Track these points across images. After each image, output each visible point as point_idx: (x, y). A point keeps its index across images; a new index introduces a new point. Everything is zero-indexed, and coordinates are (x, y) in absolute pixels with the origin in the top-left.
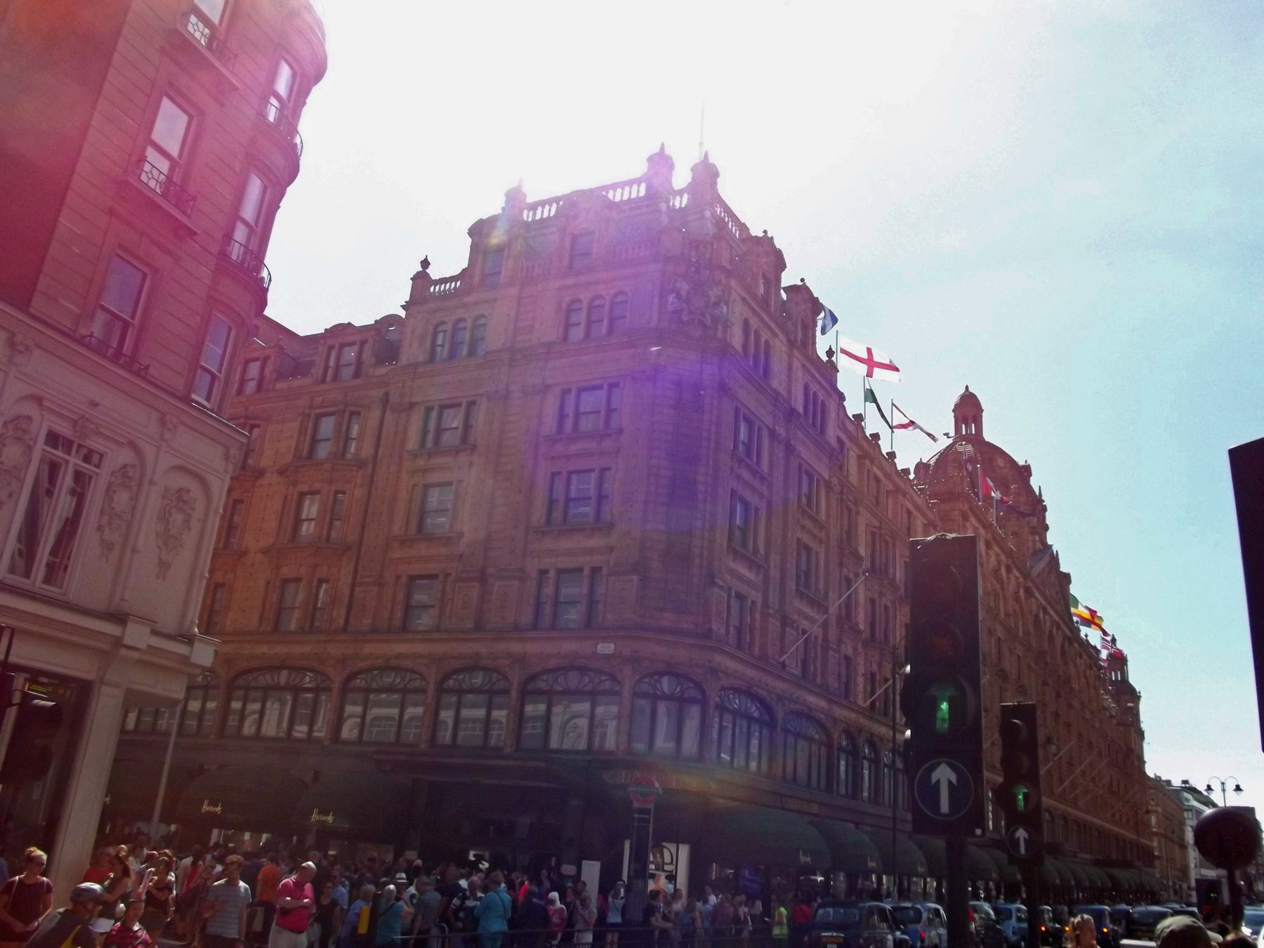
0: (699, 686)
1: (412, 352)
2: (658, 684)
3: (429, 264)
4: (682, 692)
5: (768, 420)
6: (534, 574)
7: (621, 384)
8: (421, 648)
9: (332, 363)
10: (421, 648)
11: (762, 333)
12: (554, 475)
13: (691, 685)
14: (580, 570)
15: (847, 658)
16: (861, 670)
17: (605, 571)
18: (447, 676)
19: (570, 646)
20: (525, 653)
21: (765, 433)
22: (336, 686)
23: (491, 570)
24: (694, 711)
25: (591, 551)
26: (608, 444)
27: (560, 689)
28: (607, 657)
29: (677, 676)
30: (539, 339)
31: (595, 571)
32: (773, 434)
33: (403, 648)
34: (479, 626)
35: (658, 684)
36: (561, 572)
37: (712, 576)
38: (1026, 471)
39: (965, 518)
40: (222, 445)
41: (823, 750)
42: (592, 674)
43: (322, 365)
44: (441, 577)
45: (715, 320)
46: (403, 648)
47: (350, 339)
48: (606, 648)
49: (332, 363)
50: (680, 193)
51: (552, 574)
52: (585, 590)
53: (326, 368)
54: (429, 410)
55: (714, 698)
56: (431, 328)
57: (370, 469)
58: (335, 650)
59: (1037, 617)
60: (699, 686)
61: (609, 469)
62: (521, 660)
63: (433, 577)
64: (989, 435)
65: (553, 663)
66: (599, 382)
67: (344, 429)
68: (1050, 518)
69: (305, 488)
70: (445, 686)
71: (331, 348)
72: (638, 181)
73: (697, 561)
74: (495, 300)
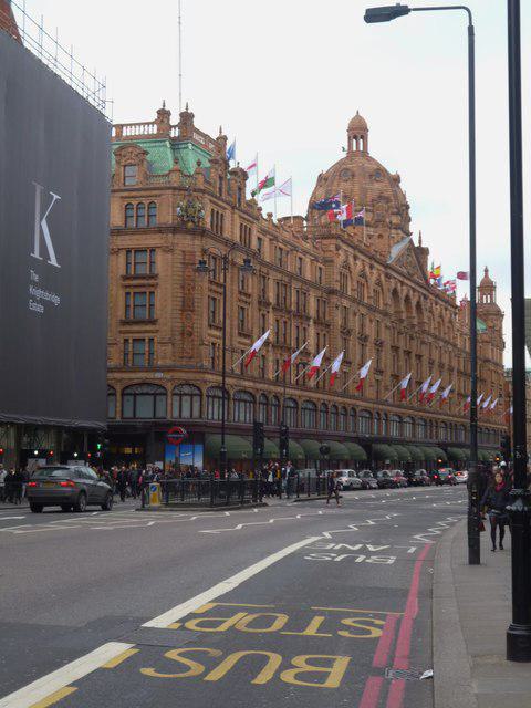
0: (199, 388)
14: (144, 340)
16: (271, 358)
24: (196, 399)
26: (152, 282)
31: (151, 340)
36: (134, 340)
37: (202, 340)
38: (396, 180)
39: (338, 248)
50: (175, 127)
55: (204, 392)
60: (199, 388)
62: (120, 380)
64: (372, 153)
72: (153, 123)
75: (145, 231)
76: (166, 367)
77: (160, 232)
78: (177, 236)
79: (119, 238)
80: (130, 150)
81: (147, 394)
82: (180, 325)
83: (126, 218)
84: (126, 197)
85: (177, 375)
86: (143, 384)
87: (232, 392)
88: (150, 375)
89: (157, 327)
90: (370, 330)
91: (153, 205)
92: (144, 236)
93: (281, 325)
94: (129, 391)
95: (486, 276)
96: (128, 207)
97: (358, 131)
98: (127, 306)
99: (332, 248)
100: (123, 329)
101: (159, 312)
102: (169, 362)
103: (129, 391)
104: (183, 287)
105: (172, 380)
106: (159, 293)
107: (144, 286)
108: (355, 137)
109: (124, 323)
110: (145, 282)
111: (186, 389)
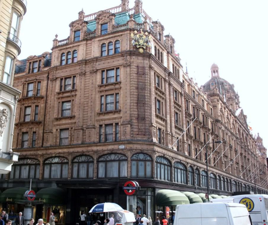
0: (150, 156)
1: (55, 62)
2: (138, 156)
3: (57, 36)
4: (145, 158)
5: (164, 76)
6: (98, 126)
7: (120, 68)
8: (66, 150)
9: (31, 68)
10: (66, 150)
11: (160, 50)
12: (102, 96)
13: (148, 156)
14: (112, 124)
15: (189, 145)
16: (193, 148)
17: (119, 124)
18: (74, 158)
19: (111, 147)
20: (97, 150)
21: (163, 80)
22: (41, 163)
23: (84, 126)
25: (115, 118)
26: (117, 86)
27: (109, 160)
28: (122, 150)
29: (144, 153)
30: (93, 56)
31: (117, 124)
32: (165, 80)
33: (60, 151)
34: (82, 143)
35: (138, 156)
39: (218, 101)
40: (14, 95)
41: (185, 172)
42: (118, 155)
43: (28, 69)
44: (70, 129)
45: (147, 47)
46: (60, 151)
47: (35, 60)
48: (122, 147)
49: (31, 68)
50: (132, 9)
51: (104, 126)
52: (114, 130)
53: (29, 69)
54: (62, 79)
56: (60, 55)
57: (45, 99)
58: (40, 153)
59: (239, 128)
61: (118, 93)
62: (96, 152)
63: (68, 129)
65: (106, 152)
66: (112, 68)
67: (36, 87)
68: (241, 99)
69: (26, 105)
70: (74, 161)
71: (30, 63)
72: (119, 7)
73: (147, 119)
74: (79, 45)
75: (113, 57)
76: (127, 140)
77: (122, 56)
78: (134, 57)
79: (98, 63)
80: (105, 15)
81: (114, 161)
82: (136, 113)
83: (102, 52)
84: (101, 40)
85: (135, 146)
86: (112, 153)
87: (173, 162)
88: (115, 147)
89: (121, 115)
90: (232, 143)
91: (118, 42)
92: (112, 60)
93: (197, 130)
94: (102, 159)
95: (258, 136)
96: (103, 46)
97: (215, 69)
98: (101, 105)
99: (216, 100)
100: (98, 118)
101: (121, 106)
102: (128, 137)
103: (102, 159)
104: (137, 88)
105: (131, 150)
106: (122, 92)
107: (112, 90)
108: (214, 72)
109: (99, 114)
110: (112, 87)
111: (141, 157)
